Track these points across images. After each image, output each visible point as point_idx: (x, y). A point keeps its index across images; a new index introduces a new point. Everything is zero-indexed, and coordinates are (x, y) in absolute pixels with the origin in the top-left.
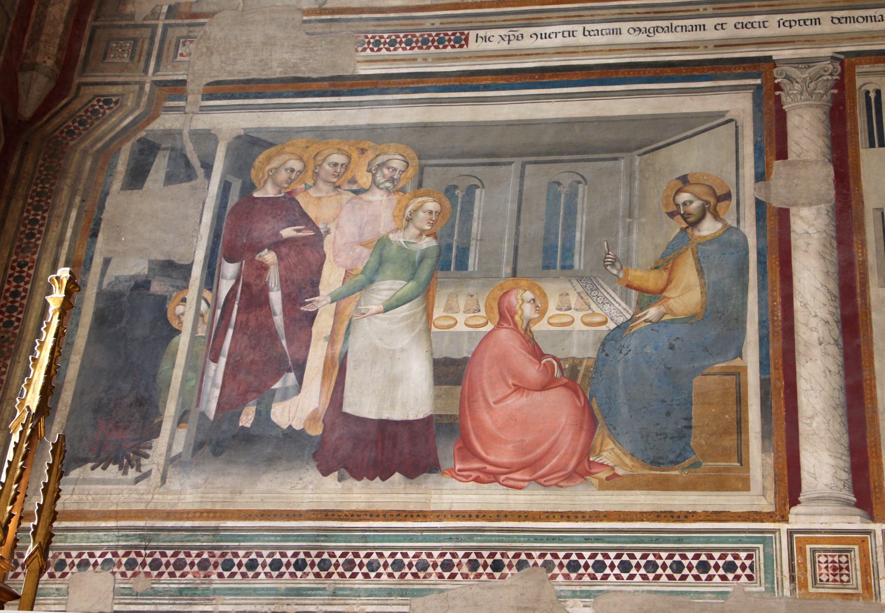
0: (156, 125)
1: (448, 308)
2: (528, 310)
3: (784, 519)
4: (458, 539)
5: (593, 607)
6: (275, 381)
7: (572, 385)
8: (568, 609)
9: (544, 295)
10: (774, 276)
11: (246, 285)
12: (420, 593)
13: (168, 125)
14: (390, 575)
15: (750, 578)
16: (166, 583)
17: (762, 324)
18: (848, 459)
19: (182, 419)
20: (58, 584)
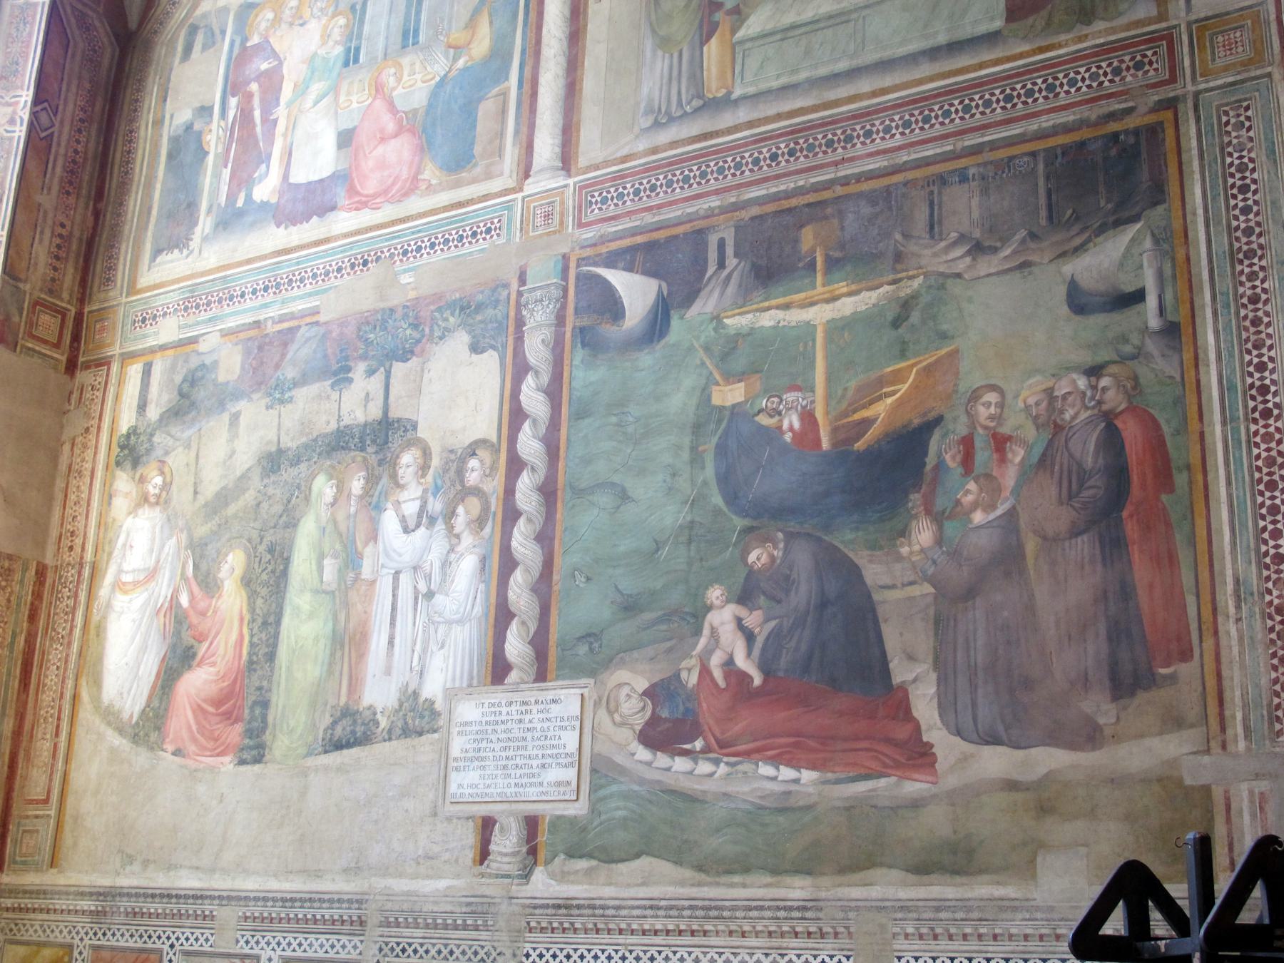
0: (198, 12)
1: (349, 94)
2: (392, 81)
3: (521, 190)
4: (345, 251)
6: (255, 172)
7: (412, 131)
9: (401, 66)
10: (533, 15)
11: (242, 110)
12: (326, 291)
13: (204, 9)
14: (311, 284)
15: (498, 235)
16: (204, 316)
17: (523, 52)
18: (560, 137)
19: (209, 211)
20: (154, 329)
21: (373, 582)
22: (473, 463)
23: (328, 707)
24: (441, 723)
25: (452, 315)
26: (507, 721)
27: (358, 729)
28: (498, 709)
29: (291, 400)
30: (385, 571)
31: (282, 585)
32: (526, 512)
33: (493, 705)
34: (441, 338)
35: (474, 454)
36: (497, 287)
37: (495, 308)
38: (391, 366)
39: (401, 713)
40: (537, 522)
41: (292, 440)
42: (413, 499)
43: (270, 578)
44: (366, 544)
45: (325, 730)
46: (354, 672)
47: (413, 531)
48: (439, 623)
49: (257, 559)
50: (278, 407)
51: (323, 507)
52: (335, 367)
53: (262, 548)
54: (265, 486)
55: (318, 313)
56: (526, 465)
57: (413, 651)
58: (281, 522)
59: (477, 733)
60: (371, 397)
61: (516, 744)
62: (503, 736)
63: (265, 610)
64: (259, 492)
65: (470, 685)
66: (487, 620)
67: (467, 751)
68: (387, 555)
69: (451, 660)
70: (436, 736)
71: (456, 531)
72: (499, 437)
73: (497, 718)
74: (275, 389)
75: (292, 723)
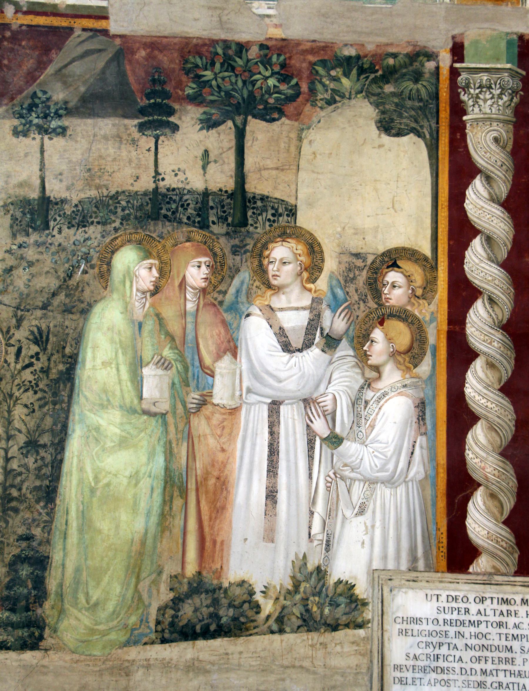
5: (276, 9)
8: (254, 10)
21: (234, 411)
22: (393, 276)
23: (164, 577)
24: (368, 615)
25: (347, 75)
26: (479, 623)
27: (221, 613)
28: (462, 606)
29: (63, 131)
30: (253, 398)
31: (64, 394)
32: (485, 353)
33: (455, 599)
34: (331, 102)
35: (395, 265)
36: (417, 54)
37: (416, 81)
38: (245, 123)
39: (298, 597)
40: (503, 372)
41: (68, 189)
42: (297, 309)
43: (39, 379)
44: (219, 357)
45: (162, 610)
46: (207, 529)
47: (300, 350)
48: (353, 480)
49: (13, 350)
50: (38, 137)
51: (136, 296)
52: (143, 102)
53: (21, 334)
54: (20, 246)
55: (106, 18)
56: (481, 293)
57: (312, 513)
58: (56, 302)
59: (430, 634)
60: (212, 157)
61: (496, 654)
62: (474, 642)
63: (32, 424)
64: (9, 252)
65: (413, 569)
66: (435, 485)
67: (416, 658)
68: (256, 376)
69: (378, 533)
70: (361, 632)
71: (373, 361)
72: (435, 249)
73: (462, 617)
74: (30, 109)
75: (96, 595)
